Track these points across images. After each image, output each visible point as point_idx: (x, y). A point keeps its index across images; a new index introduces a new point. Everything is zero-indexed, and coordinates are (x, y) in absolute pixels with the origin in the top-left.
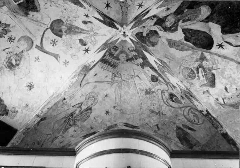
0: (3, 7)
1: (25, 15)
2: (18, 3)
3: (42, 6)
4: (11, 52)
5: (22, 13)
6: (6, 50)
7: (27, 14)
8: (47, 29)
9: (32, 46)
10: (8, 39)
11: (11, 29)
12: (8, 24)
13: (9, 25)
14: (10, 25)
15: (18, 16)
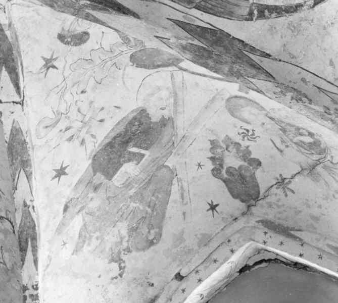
0: (170, 165)
1: (170, 124)
2: (143, 152)
3: (120, 115)
4: (282, 139)
5: (168, 131)
6: (277, 145)
7: (164, 122)
8: (181, 69)
9: (246, 98)
10: (248, 139)
11: (223, 137)
12: (211, 144)
13: (212, 142)
14: (212, 139)
15: (181, 133)
